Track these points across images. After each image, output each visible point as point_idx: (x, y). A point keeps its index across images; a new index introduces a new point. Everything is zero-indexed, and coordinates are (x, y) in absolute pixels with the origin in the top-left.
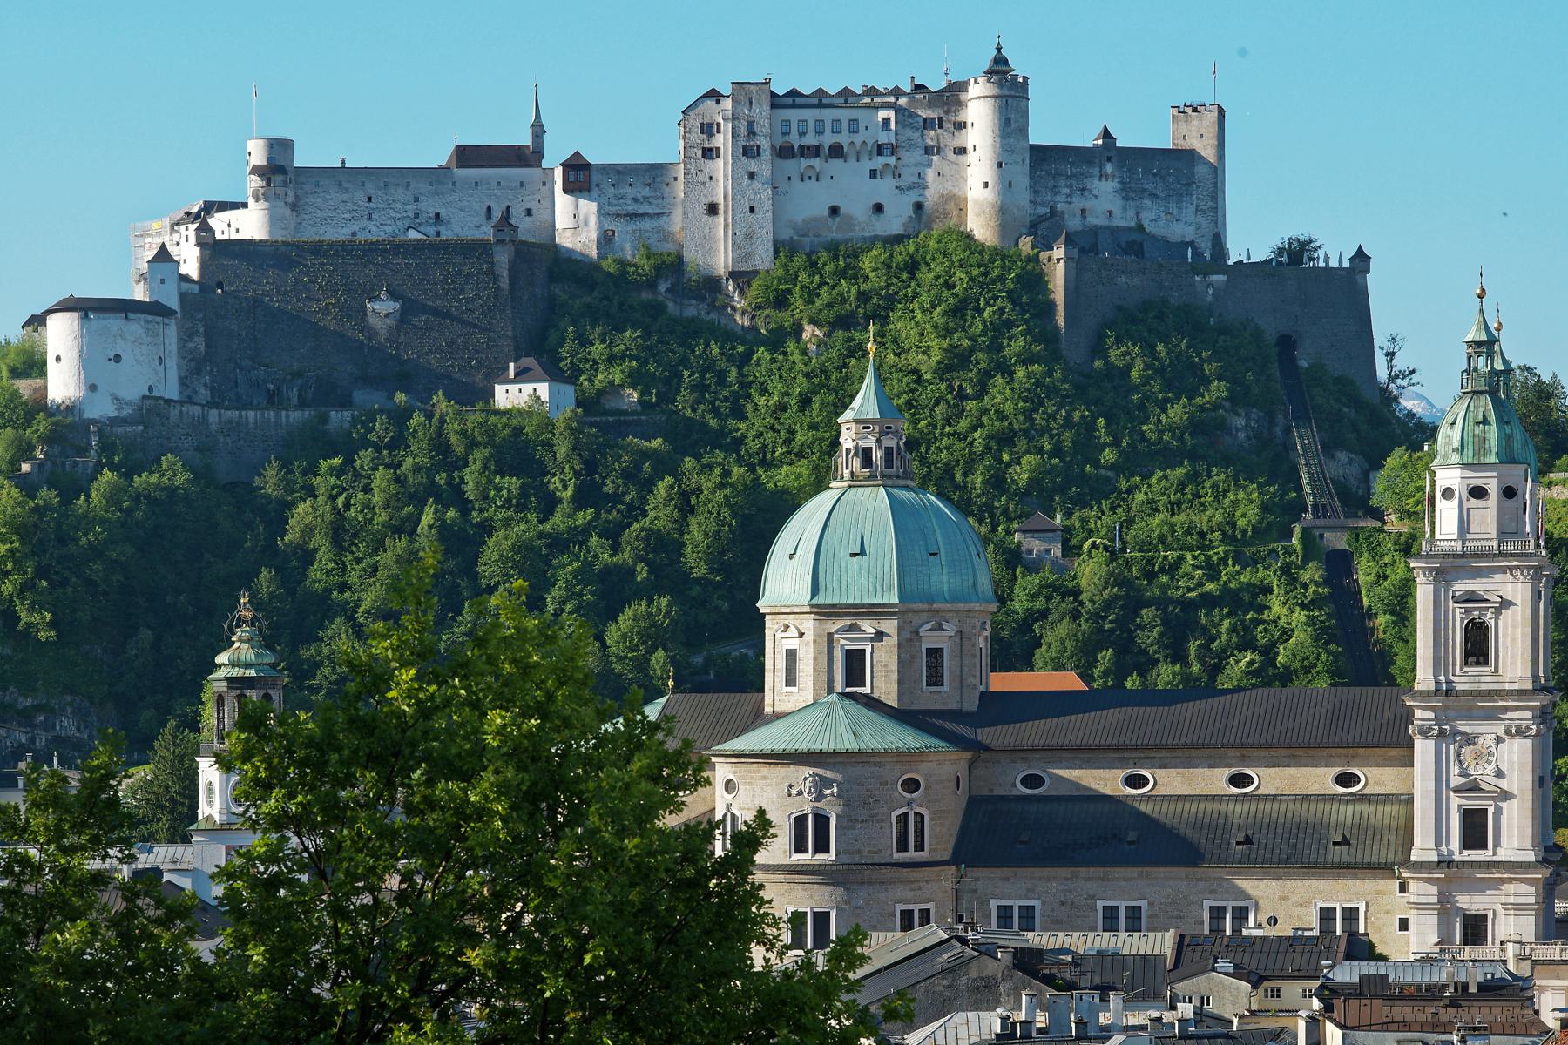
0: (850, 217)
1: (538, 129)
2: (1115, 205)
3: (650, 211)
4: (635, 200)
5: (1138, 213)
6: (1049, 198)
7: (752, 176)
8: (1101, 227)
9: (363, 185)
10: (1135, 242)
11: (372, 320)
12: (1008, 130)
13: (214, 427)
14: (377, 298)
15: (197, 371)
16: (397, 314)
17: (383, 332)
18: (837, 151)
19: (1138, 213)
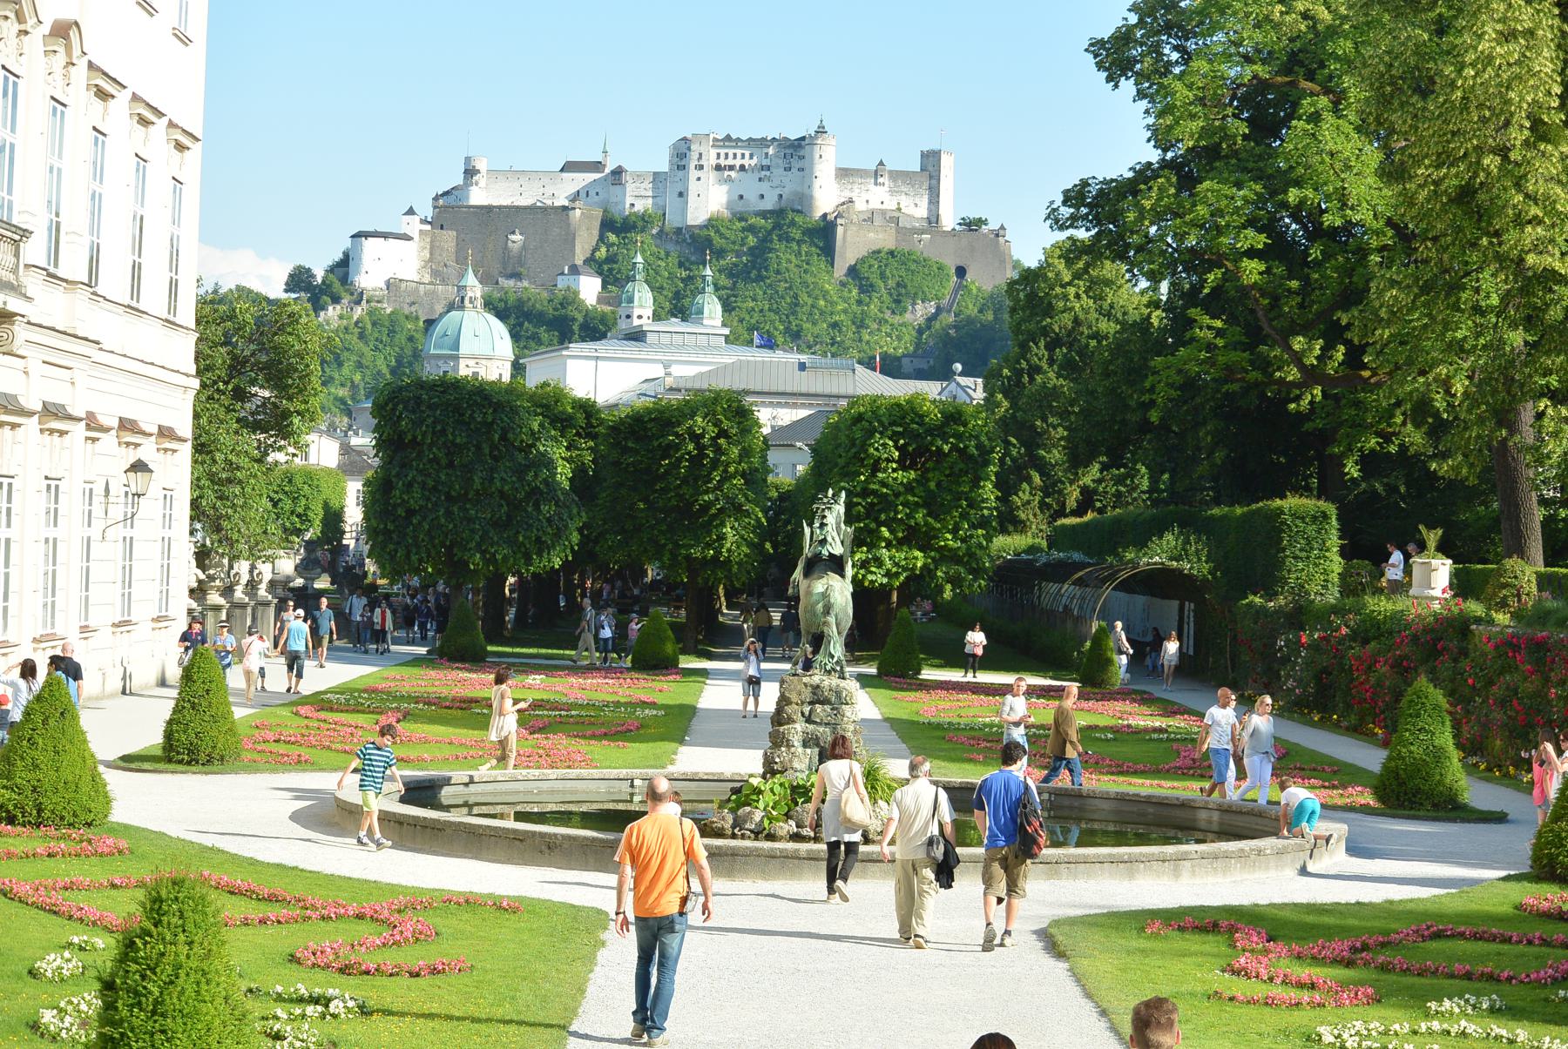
1: (605, 152)
2: (886, 197)
6: (847, 194)
7: (699, 179)
11: (510, 244)
14: (513, 233)
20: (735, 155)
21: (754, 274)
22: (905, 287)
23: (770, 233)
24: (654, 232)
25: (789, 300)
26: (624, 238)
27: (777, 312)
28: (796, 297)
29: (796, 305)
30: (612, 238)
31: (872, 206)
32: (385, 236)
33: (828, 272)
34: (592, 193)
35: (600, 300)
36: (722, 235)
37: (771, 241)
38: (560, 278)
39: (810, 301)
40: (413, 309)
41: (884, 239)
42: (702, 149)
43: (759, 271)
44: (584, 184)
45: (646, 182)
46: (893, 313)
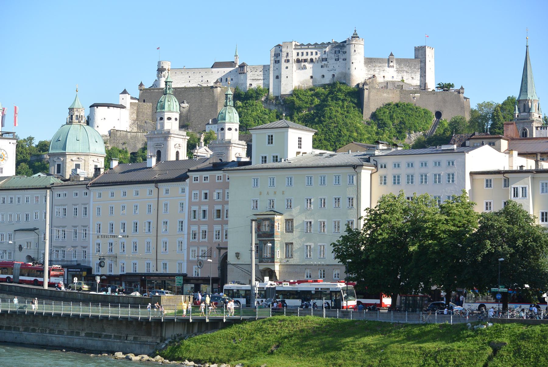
2: (395, 74)
5: (403, 78)
6: (372, 73)
7: (287, 68)
12: (355, 53)
13: (129, 137)
14: (183, 102)
17: (184, 112)
19: (403, 78)
20: (307, 53)
21: (316, 120)
22: (404, 124)
23: (327, 96)
24: (263, 99)
25: (336, 133)
26: (245, 104)
27: (328, 140)
28: (340, 131)
29: (340, 136)
30: (239, 103)
32: (108, 106)
33: (359, 117)
34: (229, 79)
36: (300, 99)
37: (327, 101)
38: (207, 126)
39: (348, 133)
40: (124, 147)
41: (393, 97)
42: (288, 50)
43: (320, 118)
44: (224, 74)
45: (258, 71)
46: (397, 139)
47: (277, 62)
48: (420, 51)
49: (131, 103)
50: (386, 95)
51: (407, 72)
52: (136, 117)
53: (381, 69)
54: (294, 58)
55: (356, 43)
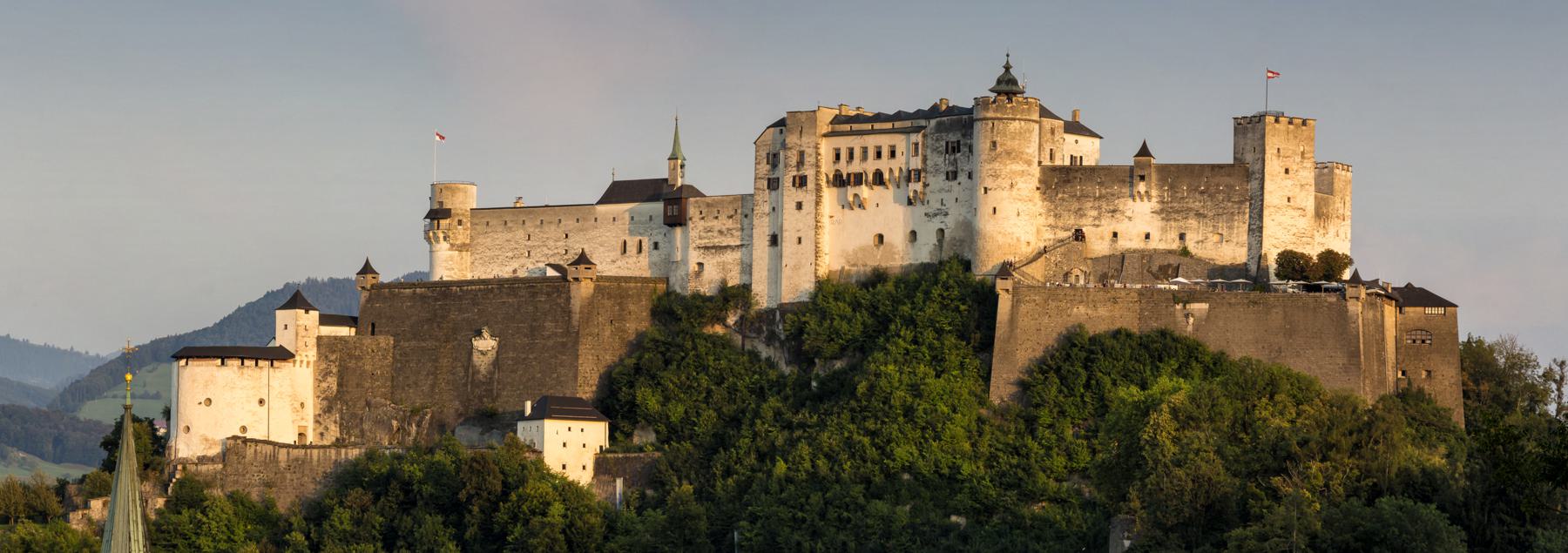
0: (892, 246)
2: (1154, 226)
3: (732, 244)
4: (721, 232)
5: (1182, 237)
6: (1072, 221)
7: (799, 206)
8: (1135, 251)
9: (524, 221)
10: (1169, 265)
11: (476, 358)
13: (283, 465)
14: (479, 334)
15: (328, 410)
16: (494, 352)
18: (879, 179)
19: (1182, 237)
31: (1124, 244)
35: (603, 465)
38: (521, 425)
45: (723, 217)
47: (773, 184)
48: (1250, 135)
49: (319, 338)
50: (1082, 309)
51: (1199, 215)
52: (335, 388)
53: (1104, 206)
54: (823, 169)
55: (999, 115)
